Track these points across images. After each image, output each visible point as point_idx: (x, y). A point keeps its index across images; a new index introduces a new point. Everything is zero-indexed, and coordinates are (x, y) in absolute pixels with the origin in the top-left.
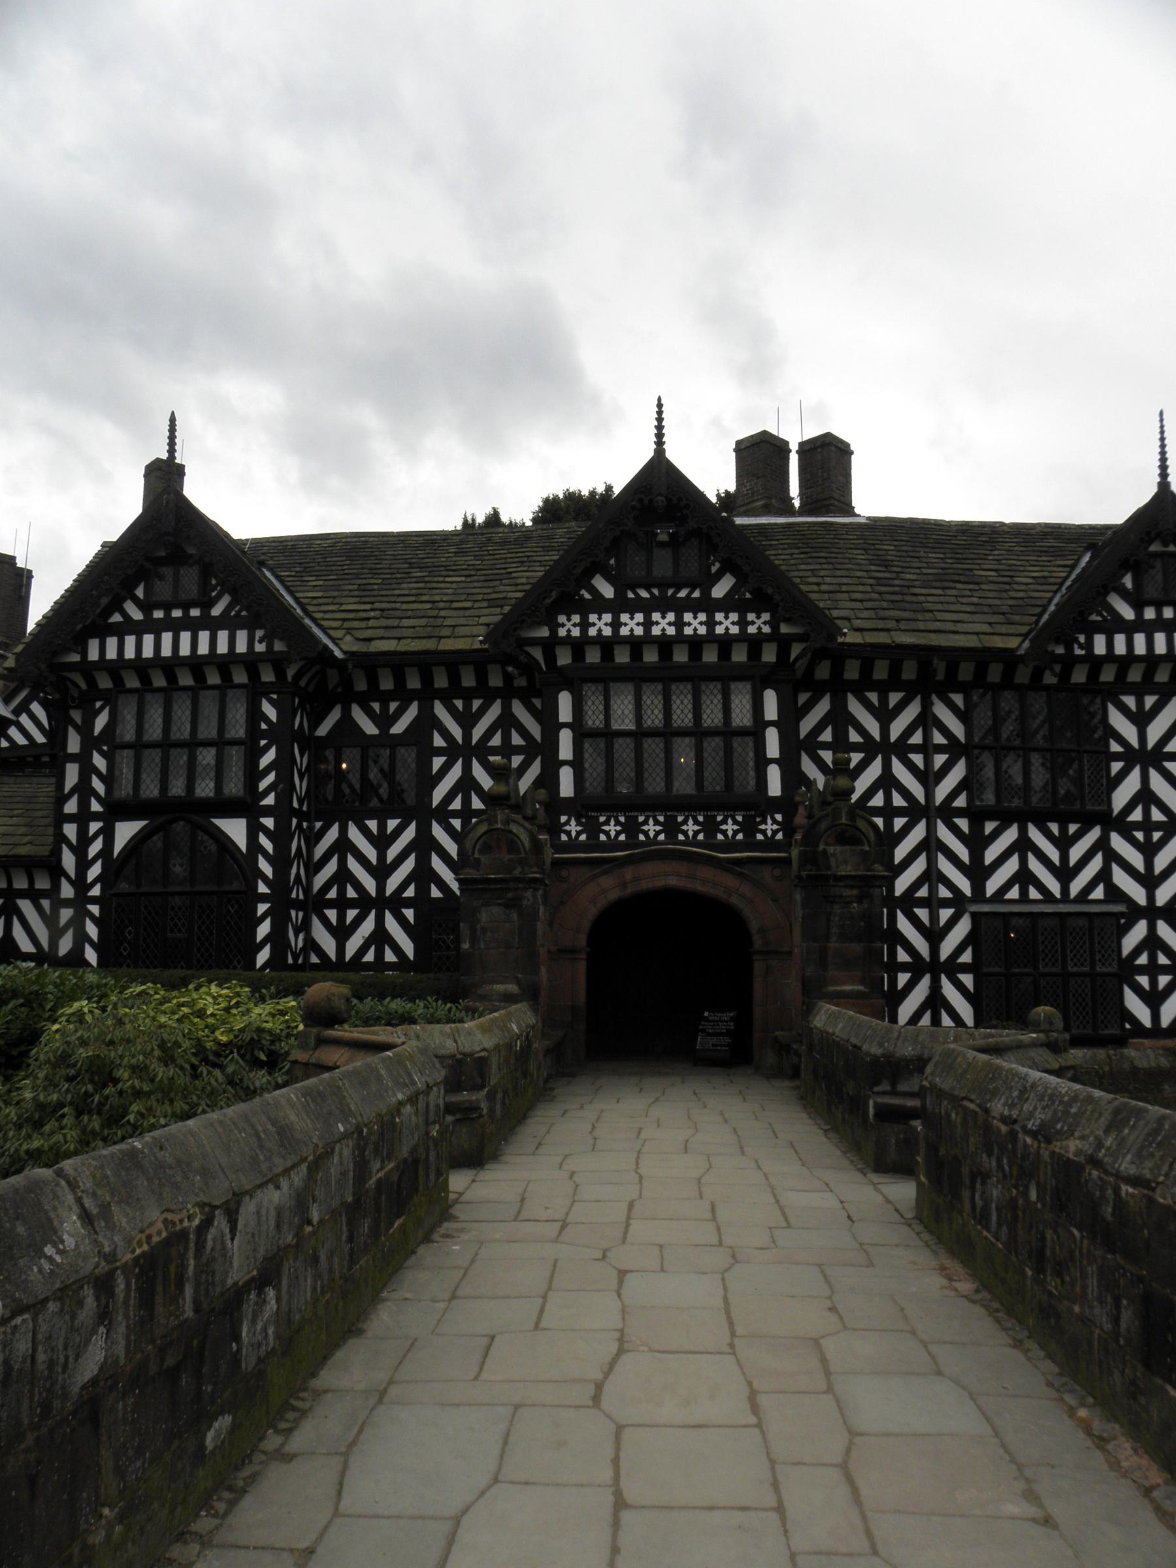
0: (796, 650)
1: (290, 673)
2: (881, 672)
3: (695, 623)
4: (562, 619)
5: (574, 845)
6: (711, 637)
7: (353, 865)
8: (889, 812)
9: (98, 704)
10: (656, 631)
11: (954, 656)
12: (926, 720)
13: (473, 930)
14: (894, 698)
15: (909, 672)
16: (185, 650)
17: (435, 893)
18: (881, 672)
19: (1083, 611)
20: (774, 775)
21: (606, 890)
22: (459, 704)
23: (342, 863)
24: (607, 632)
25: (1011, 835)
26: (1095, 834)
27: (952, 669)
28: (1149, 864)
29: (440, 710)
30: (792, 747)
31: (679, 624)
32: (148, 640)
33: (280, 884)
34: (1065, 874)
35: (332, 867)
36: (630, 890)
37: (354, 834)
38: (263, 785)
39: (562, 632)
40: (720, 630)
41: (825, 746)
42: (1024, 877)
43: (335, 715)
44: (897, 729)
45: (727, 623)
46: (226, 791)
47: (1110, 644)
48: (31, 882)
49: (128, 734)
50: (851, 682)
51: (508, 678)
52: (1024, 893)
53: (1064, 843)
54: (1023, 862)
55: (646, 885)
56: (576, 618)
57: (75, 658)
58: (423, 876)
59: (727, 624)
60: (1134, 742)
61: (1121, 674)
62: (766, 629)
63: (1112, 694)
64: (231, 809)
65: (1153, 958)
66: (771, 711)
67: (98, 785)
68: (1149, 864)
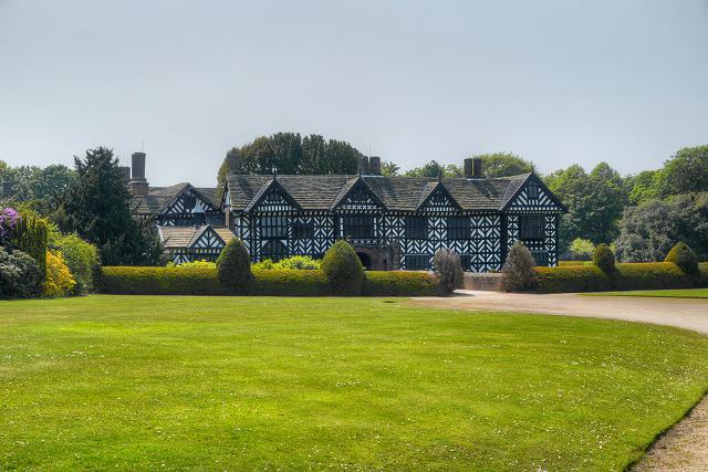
12: (398, 222)
34: (420, 249)
42: (414, 249)
49: (263, 224)
53: (420, 244)
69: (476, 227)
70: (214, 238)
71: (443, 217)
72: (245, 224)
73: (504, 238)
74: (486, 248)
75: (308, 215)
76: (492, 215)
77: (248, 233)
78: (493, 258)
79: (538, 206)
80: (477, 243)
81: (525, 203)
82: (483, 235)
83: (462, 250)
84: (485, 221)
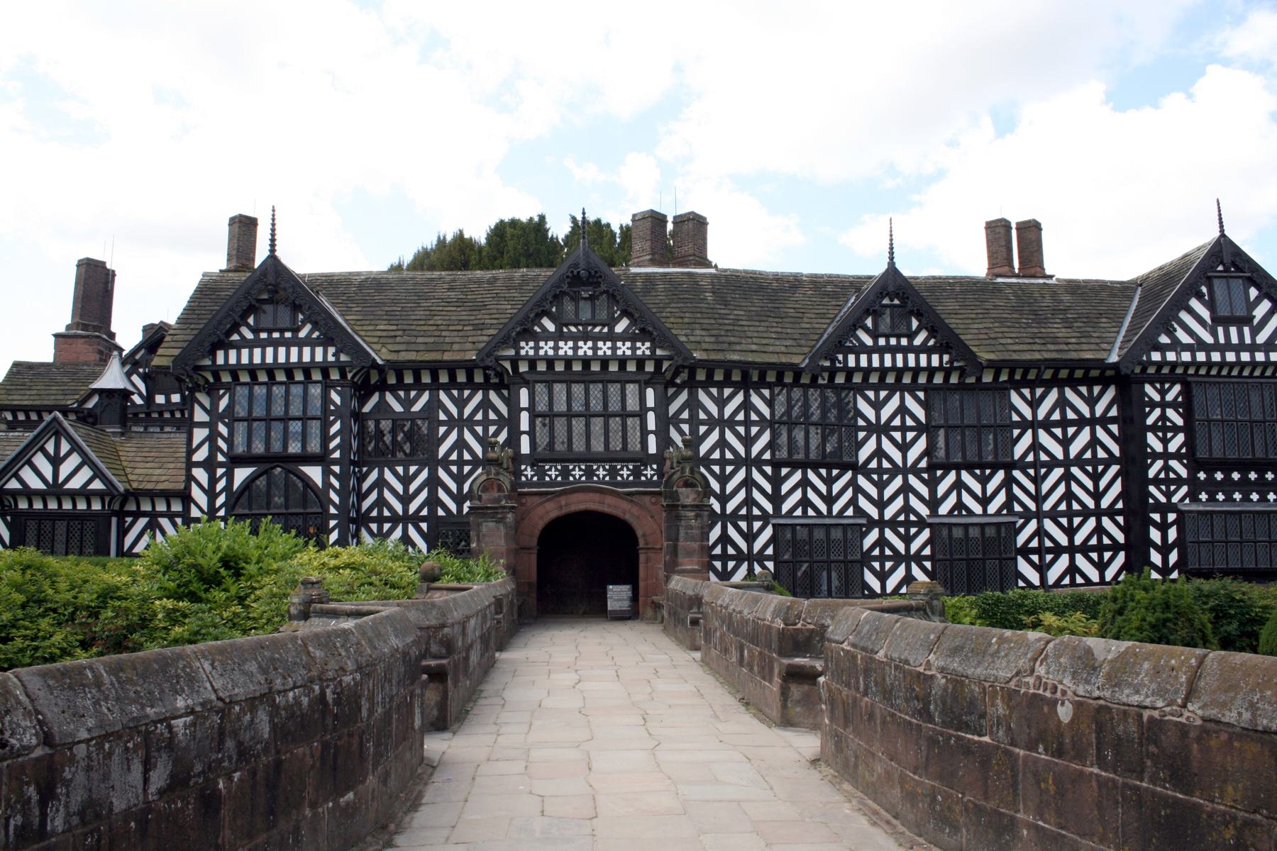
0: (665, 365)
1: (349, 376)
2: (719, 376)
3: (605, 348)
4: (523, 344)
5: (529, 483)
6: (614, 357)
7: (388, 495)
8: (723, 462)
9: (221, 392)
10: (581, 352)
11: (763, 369)
12: (747, 406)
13: (478, 536)
14: (727, 392)
15: (736, 377)
16: (282, 359)
17: (441, 513)
18: (719, 376)
19: (841, 342)
20: (652, 439)
21: (551, 511)
22: (455, 392)
23: (381, 494)
24: (551, 352)
25: (798, 476)
26: (849, 475)
27: (762, 376)
28: (881, 494)
29: (443, 396)
30: (665, 421)
31: (595, 348)
32: (257, 352)
33: (342, 508)
34: (830, 500)
35: (374, 496)
36: (565, 511)
37: (388, 475)
38: (332, 445)
39: (523, 352)
40: (619, 352)
41: (684, 421)
42: (805, 503)
43: (375, 398)
44: (728, 411)
45: (624, 348)
46: (309, 449)
47: (858, 361)
48: (169, 506)
49: (241, 411)
50: (701, 382)
51: (487, 377)
52: (805, 512)
53: (829, 482)
54: (805, 493)
55: (574, 508)
56: (531, 344)
57: (208, 362)
58: (433, 502)
59: (624, 349)
60: (873, 420)
61: (866, 379)
62: (648, 352)
63: (860, 389)
65: (882, 551)
66: (650, 402)
67: (222, 444)
68: (881, 494)
69: (1034, 425)
70: (75, 460)
71: (912, 389)
73: (1133, 461)
75: (419, 386)
76: (1090, 383)
78: (1099, 530)
79: (1253, 348)
80: (1037, 481)
81: (1209, 339)
82: (1058, 452)
83: (985, 501)
84: (1062, 403)
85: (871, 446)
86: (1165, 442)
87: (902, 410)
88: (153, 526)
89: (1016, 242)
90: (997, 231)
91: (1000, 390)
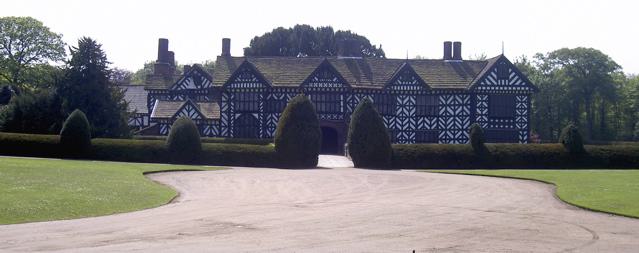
59: (335, 85)
64: (255, 112)
70: (193, 111)
72: (223, 99)
74: (454, 125)
77: (227, 107)
79: (509, 86)
83: (430, 126)
84: (455, 99)
85: (400, 110)
86: (482, 111)
87: (409, 101)
88: (211, 128)
89: (453, 49)
90: (447, 45)
91: (437, 95)
